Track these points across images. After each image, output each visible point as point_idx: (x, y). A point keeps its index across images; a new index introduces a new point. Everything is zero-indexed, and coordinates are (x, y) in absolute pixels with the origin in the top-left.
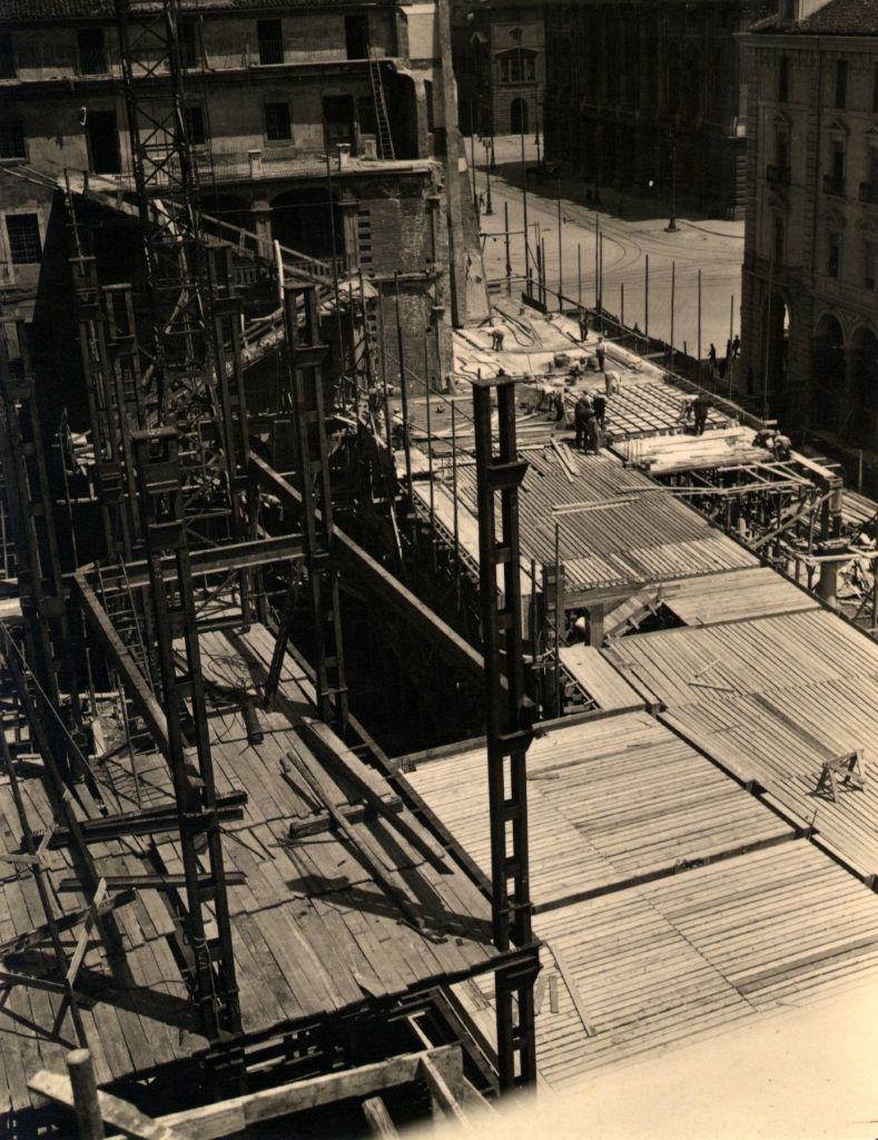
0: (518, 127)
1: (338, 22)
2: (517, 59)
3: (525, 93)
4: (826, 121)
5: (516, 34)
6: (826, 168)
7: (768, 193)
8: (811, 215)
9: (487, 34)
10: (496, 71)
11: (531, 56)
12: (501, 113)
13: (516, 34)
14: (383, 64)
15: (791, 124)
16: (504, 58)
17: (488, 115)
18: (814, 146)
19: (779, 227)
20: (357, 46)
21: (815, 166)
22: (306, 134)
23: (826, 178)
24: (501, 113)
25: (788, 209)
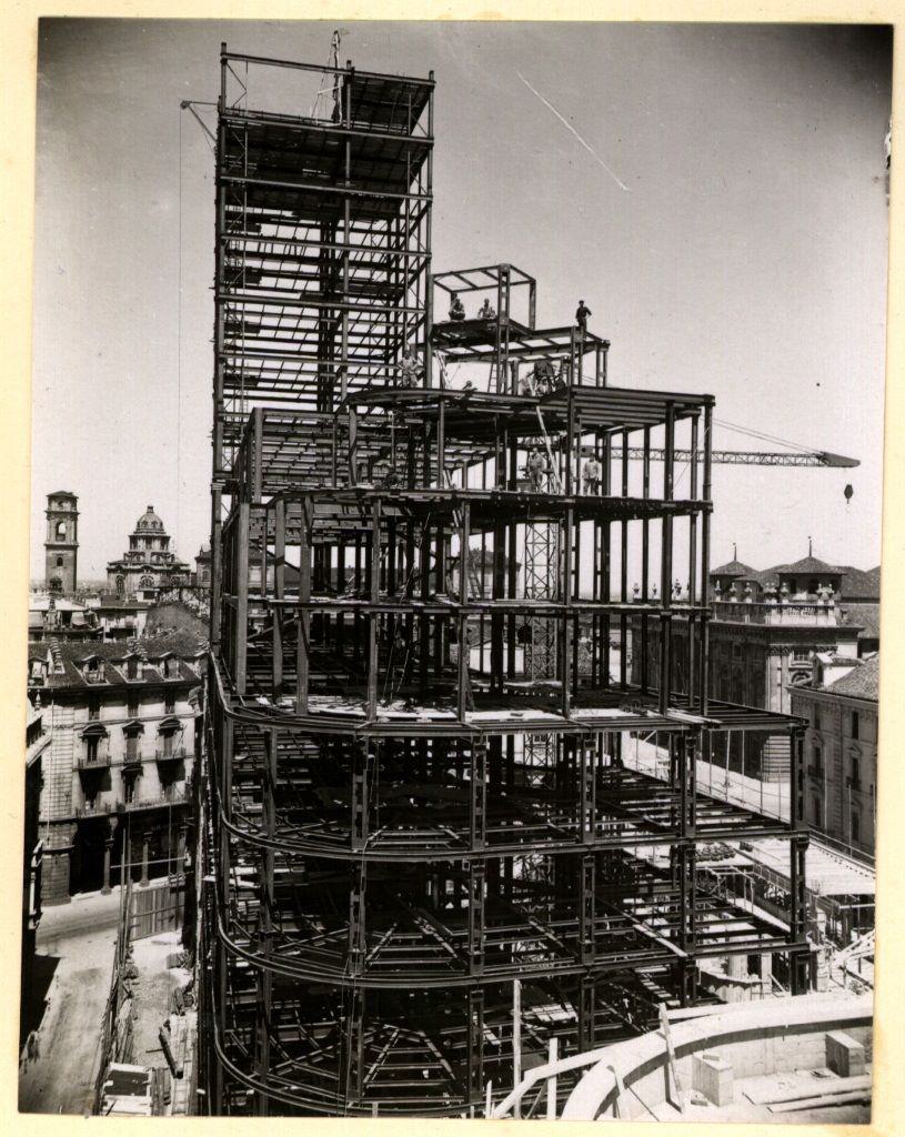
6: (848, 772)
8: (838, 799)
15: (823, 743)
18: (838, 755)
21: (840, 769)
23: (848, 778)
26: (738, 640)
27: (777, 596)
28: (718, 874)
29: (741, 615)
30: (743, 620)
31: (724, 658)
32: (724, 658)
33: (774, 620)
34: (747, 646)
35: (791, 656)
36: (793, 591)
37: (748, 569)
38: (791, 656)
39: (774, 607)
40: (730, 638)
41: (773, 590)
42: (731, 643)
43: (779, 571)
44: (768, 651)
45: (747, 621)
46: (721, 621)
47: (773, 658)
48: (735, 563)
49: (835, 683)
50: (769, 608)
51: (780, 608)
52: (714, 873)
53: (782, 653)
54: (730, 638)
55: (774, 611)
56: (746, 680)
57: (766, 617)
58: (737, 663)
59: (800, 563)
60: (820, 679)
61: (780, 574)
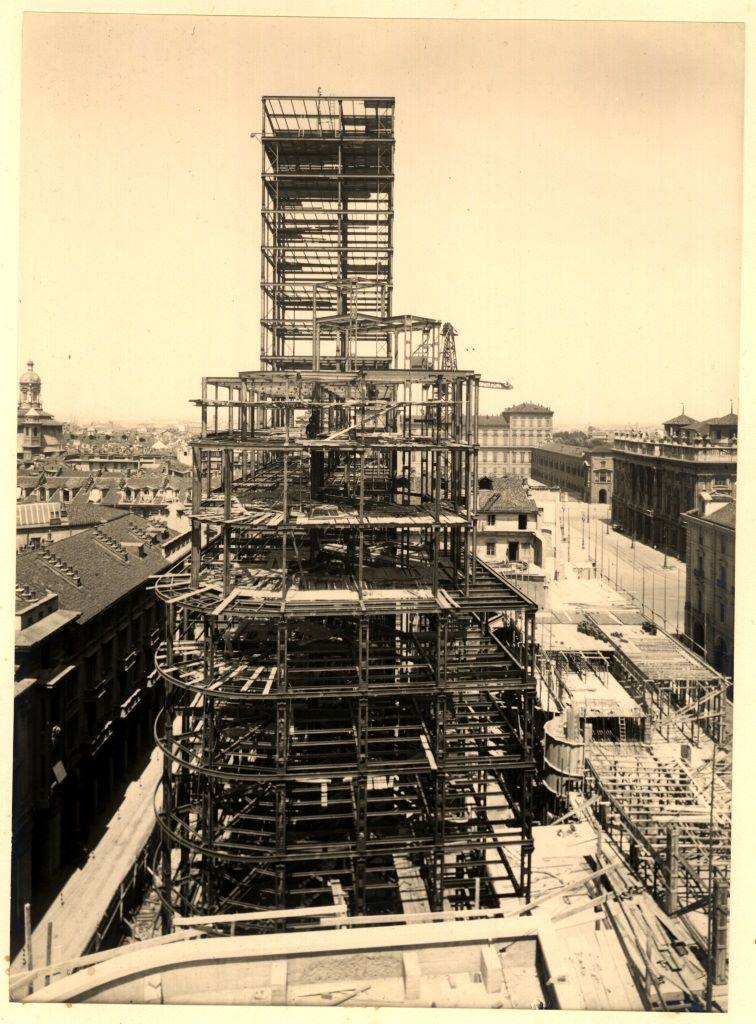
0: (602, 499)
1: (517, 517)
2: (603, 473)
3: (605, 487)
4: (718, 557)
5: (603, 463)
6: (718, 577)
7: (695, 580)
9: (590, 461)
10: (595, 477)
11: (609, 472)
12: (595, 495)
13: (603, 463)
14: (531, 533)
16: (597, 472)
17: (589, 495)
18: (713, 565)
19: (700, 594)
20: (523, 525)
21: (714, 574)
22: (502, 549)
24: (595, 495)
25: (703, 588)
26: (677, 470)
27: (706, 442)
28: (586, 658)
29: (680, 454)
30: (680, 457)
31: (669, 481)
32: (669, 481)
33: (700, 458)
34: (684, 475)
35: (713, 482)
36: (719, 437)
37: (691, 421)
38: (713, 482)
39: (701, 449)
40: (672, 469)
41: (700, 438)
42: (673, 472)
43: (712, 423)
44: (697, 479)
45: (683, 458)
46: (666, 457)
47: (700, 484)
48: (683, 417)
49: (714, 513)
50: (697, 451)
51: (705, 451)
52: (584, 657)
53: (706, 480)
54: (672, 469)
55: (700, 453)
56: (682, 496)
57: (696, 457)
58: (677, 484)
59: (724, 418)
60: (703, 511)
61: (711, 426)
